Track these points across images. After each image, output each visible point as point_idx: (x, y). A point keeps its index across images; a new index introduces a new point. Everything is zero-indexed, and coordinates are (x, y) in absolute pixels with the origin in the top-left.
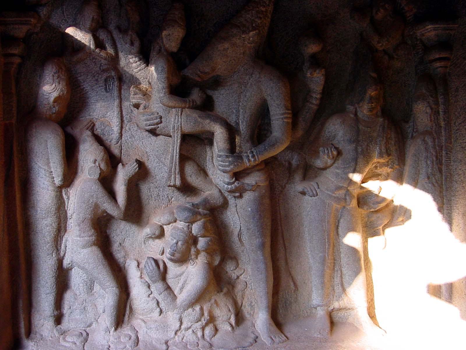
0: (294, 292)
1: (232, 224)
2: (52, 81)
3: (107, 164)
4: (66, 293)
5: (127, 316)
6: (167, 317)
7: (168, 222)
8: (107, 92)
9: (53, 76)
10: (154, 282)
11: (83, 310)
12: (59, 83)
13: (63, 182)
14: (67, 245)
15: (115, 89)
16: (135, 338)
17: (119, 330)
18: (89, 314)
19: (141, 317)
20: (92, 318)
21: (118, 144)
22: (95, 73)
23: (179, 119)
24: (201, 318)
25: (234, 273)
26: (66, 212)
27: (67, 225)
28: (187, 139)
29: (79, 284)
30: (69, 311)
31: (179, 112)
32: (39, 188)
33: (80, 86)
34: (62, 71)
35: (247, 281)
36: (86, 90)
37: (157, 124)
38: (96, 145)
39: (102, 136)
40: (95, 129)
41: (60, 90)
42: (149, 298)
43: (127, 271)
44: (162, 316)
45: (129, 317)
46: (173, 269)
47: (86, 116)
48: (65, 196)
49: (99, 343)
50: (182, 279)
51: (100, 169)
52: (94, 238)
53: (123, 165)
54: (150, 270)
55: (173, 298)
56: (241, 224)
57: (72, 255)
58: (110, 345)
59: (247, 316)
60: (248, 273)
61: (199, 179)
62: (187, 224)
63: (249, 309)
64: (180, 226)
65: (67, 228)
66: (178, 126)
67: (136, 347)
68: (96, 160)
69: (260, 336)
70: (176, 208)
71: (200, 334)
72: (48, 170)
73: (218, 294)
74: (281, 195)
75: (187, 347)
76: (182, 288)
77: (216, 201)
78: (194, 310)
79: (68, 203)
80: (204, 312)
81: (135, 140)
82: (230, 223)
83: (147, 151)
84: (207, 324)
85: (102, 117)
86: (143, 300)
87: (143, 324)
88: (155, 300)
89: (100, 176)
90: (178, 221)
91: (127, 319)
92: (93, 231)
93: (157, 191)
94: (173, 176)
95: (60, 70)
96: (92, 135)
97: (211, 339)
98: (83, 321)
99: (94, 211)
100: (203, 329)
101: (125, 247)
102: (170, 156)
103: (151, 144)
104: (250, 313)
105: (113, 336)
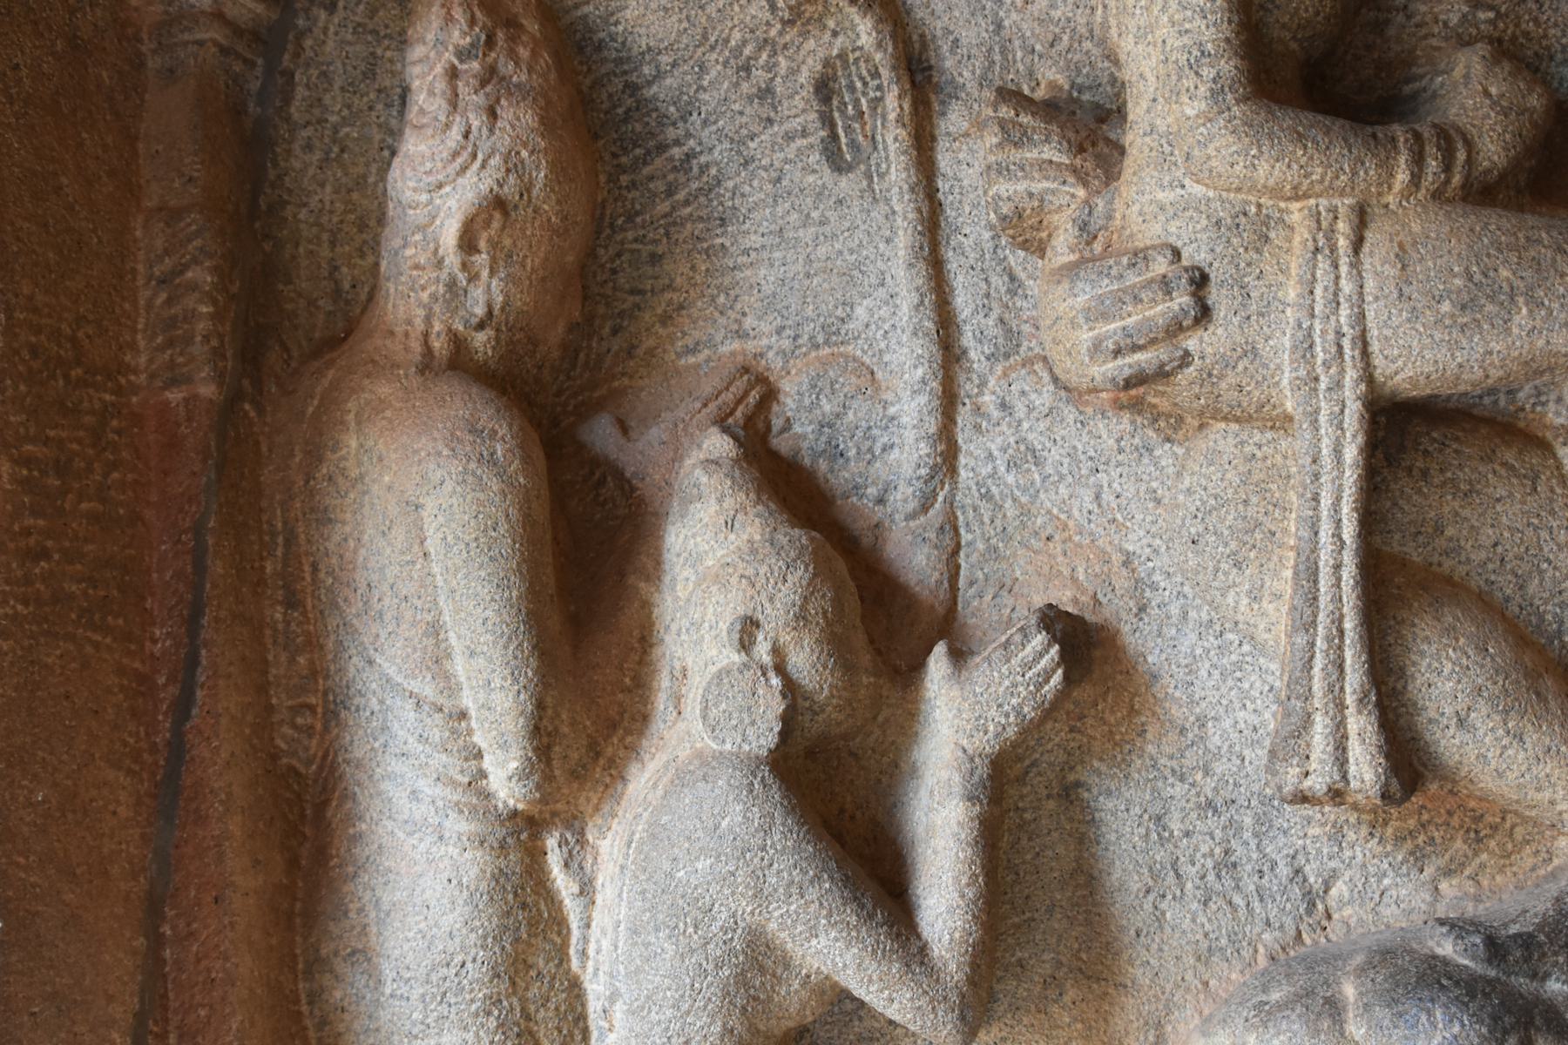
2: (444, 105)
3: (836, 643)
8: (837, 163)
9: (453, 74)
12: (492, 114)
13: (538, 787)
15: (890, 140)
21: (931, 512)
22: (744, 42)
23: (1343, 282)
26: (575, 988)
28: (1405, 433)
31: (1342, 226)
32: (389, 824)
33: (662, 148)
34: (512, 40)
36: (704, 169)
37: (1175, 329)
38: (753, 528)
39: (823, 465)
40: (777, 423)
41: (495, 161)
47: (719, 338)
48: (563, 882)
51: (791, 688)
53: (959, 656)
61: (1531, 738)
66: (1340, 334)
68: (748, 629)
70: (1361, 971)
72: (441, 701)
79: (588, 926)
81: (1045, 479)
83: (1131, 548)
85: (820, 339)
89: (784, 735)
93: (1218, 834)
94: (1321, 726)
95: (500, 35)
96: (736, 461)
99: (746, 985)
102: (1289, 573)
103: (1158, 502)
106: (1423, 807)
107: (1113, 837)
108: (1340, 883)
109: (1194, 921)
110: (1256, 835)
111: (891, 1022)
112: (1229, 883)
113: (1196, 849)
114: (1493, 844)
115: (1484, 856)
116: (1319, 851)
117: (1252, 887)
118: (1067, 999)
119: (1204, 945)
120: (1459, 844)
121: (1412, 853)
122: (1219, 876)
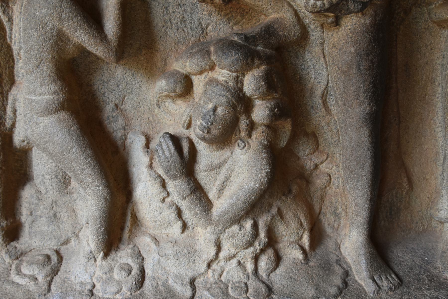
0: (407, 193)
1: (313, 77)
4: (23, 189)
5: (127, 231)
6: (195, 235)
7: (199, 70)
10: (174, 177)
11: (53, 218)
14: (17, 108)
16: (138, 272)
17: (113, 255)
18: (64, 224)
19: (151, 231)
20: (68, 231)
24: (254, 241)
25: (311, 160)
26: (9, 48)
27: (15, 73)
29: (43, 175)
30: (30, 219)
35: (332, 173)
42: (164, 205)
43: (128, 153)
44: (185, 233)
45: (131, 231)
46: (206, 155)
49: (77, 278)
50: (222, 174)
52: (61, 97)
54: (165, 158)
55: (206, 206)
56: (328, 76)
57: (25, 127)
58: (96, 283)
59: (329, 230)
60: (335, 160)
62: (234, 74)
63: (331, 220)
64: (221, 79)
65: (16, 78)
67: (139, 290)
69: (351, 270)
70: (215, 44)
71: (250, 266)
73: (283, 198)
74: (401, 27)
75: (227, 295)
76: (223, 189)
77: (289, 33)
78: (241, 227)
79: (12, 30)
80: (260, 230)
82: (308, 74)
84: (262, 251)
86: (153, 207)
87: (153, 246)
88: (174, 207)
90: (217, 68)
91: (128, 235)
92: (59, 82)
93: (181, 12)
97: (269, 275)
98: (54, 236)
99: (58, 45)
100: (256, 259)
101: (126, 110)
104: (333, 226)
105: (101, 267)
106: (231, 7)
107: (155, 12)
108: (210, 27)
109: (174, 34)
110: (190, 13)
111: (98, 58)
112: (183, 25)
113: (176, 16)
114: (247, 17)
115: (244, 20)
116: (205, 18)
117: (189, 27)
118: (143, 53)
119: (177, 41)
120: (239, 17)
121: (228, 19)
122: (181, 23)
